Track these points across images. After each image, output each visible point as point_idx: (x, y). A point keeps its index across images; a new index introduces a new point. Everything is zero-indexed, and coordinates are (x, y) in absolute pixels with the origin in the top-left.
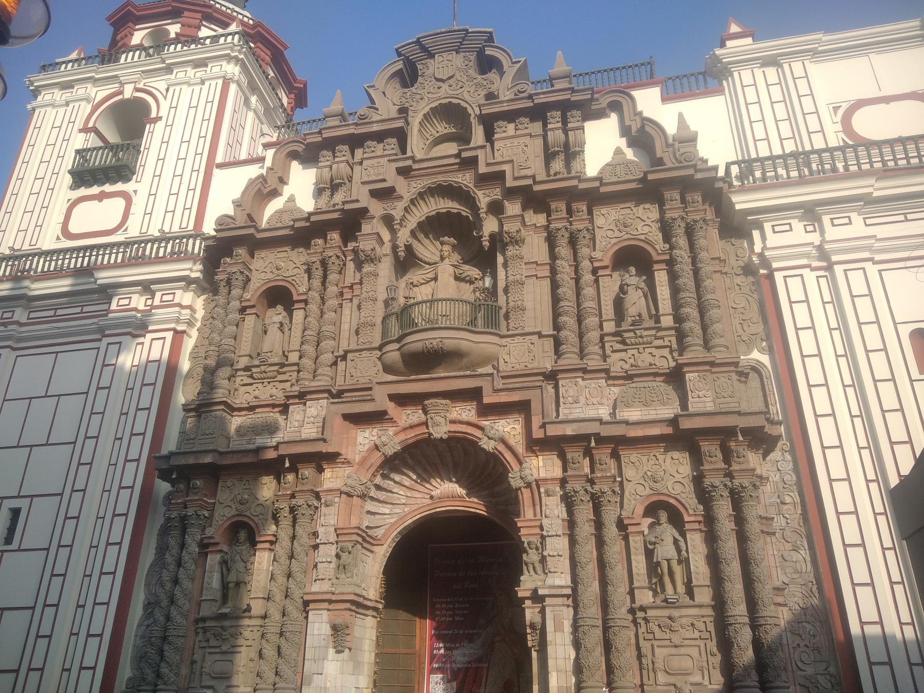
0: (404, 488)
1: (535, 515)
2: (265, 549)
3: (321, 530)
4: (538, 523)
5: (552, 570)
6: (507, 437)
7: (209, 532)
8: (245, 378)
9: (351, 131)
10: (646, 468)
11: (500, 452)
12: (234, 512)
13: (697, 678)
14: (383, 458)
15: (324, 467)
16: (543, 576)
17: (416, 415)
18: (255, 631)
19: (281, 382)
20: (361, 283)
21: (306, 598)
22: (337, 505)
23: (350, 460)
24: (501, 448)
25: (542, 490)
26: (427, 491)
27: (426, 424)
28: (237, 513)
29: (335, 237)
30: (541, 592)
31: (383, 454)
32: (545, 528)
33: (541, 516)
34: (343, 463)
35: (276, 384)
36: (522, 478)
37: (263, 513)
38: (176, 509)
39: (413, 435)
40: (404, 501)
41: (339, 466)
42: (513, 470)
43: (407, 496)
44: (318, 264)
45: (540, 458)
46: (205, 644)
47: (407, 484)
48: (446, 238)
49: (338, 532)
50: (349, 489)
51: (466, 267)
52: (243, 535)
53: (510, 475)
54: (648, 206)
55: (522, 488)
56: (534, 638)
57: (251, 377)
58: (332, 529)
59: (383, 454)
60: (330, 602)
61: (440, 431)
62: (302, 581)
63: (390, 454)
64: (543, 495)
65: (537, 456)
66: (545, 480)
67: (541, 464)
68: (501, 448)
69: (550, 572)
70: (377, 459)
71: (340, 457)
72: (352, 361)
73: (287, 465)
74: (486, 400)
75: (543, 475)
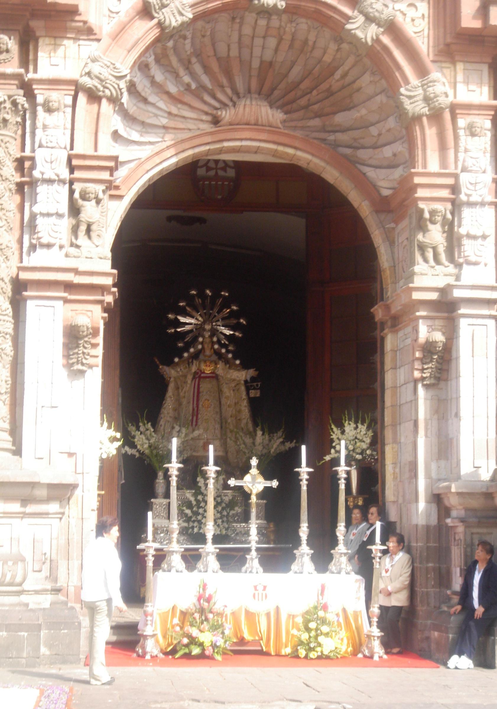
0: (165, 97)
1: (443, 163)
3: (40, 155)
4: (450, 181)
5: (473, 259)
6: (399, 18)
11: (386, 48)
14: (156, 32)
15: (38, 34)
16: (451, 269)
21: (23, 276)
22: (70, 110)
23: (94, 27)
24: (386, 40)
25: (462, 122)
26: (206, 108)
30: (457, 293)
31: (160, 24)
32: (464, 190)
33: (456, 168)
34: (79, 31)
36: (427, 99)
40: (164, 121)
41: (68, 36)
42: (407, 82)
43: (170, 113)
45: (460, 66)
47: (173, 89)
49: (75, 162)
50: (96, 83)
53: (402, 90)
55: (425, 119)
56: (426, 367)
59: (160, 24)
60: (69, 286)
62: (9, 245)
63: (174, 24)
64: (461, 133)
65: (454, 63)
66: (469, 107)
67: (460, 77)
68: (386, 40)
69: (469, 263)
71: (77, 18)
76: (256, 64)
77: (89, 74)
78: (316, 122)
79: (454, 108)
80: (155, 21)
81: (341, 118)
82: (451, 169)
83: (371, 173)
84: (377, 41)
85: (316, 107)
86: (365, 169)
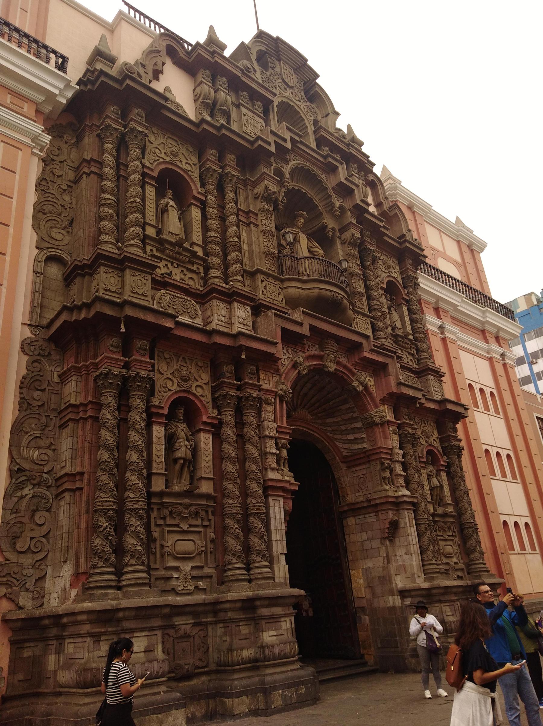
2: (209, 431)
4: (390, 452)
7: (156, 401)
8: (155, 250)
9: (240, 75)
10: (422, 428)
12: (175, 388)
13: (455, 560)
17: (315, 348)
18: (210, 513)
19: (189, 270)
20: (256, 215)
25: (391, 429)
27: (321, 358)
28: (179, 389)
29: (230, 159)
31: (299, 372)
35: (185, 270)
37: (204, 395)
38: (113, 365)
39: (315, 363)
44: (216, 175)
45: (386, 406)
46: (162, 522)
48: (305, 213)
51: (317, 245)
52: (181, 412)
54: (395, 260)
57: (162, 251)
58: (275, 425)
61: (332, 367)
63: (304, 373)
65: (384, 404)
70: (294, 374)
72: (262, 281)
73: (243, 357)
74: (367, 355)
75: (388, 418)
76: (301, 394)
77: (281, 390)
78: (319, 421)
79: (389, 422)
80: (297, 371)
81: (328, 420)
82: (391, 447)
83: (340, 445)
84: (362, 391)
85: (319, 415)
86: (337, 443)
